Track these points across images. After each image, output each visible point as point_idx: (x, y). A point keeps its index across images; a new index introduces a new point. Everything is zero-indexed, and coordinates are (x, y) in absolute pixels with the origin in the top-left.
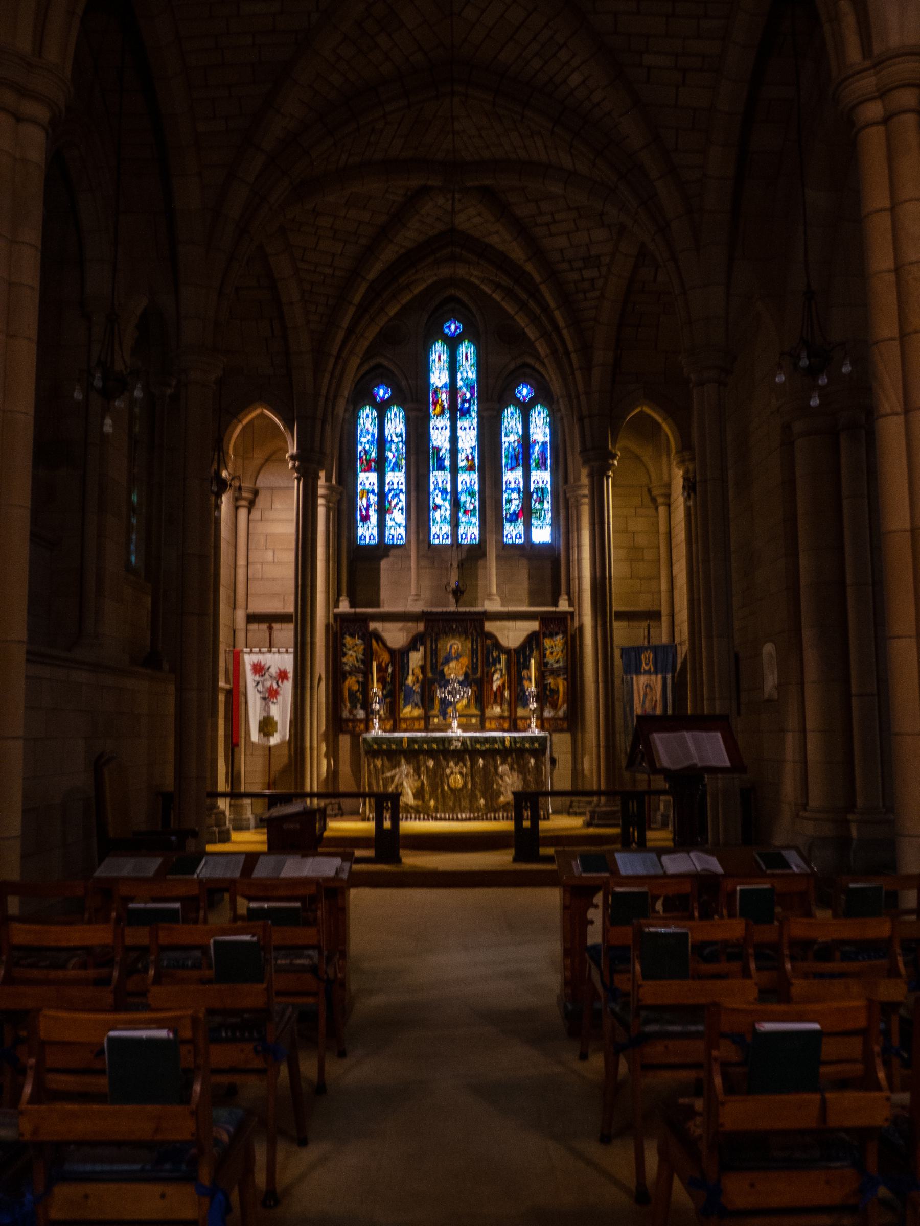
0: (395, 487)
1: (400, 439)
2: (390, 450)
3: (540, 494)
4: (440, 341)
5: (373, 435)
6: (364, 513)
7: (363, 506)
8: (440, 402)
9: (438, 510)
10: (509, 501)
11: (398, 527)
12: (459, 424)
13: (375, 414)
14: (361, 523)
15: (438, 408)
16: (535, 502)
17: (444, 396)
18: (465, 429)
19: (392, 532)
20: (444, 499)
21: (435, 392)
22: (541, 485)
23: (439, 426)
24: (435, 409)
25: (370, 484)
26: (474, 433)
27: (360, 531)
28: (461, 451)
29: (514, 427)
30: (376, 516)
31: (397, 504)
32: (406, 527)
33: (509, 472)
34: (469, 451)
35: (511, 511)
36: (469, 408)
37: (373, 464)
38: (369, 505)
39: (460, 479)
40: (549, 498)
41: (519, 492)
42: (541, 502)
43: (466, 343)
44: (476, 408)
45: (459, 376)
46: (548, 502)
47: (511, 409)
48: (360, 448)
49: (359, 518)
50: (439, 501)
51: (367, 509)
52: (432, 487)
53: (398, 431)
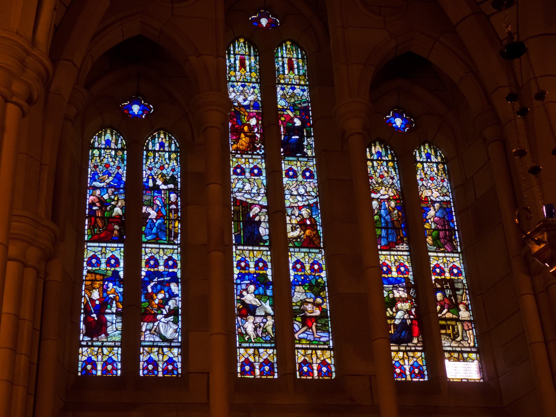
0: (161, 268)
1: (171, 186)
2: (151, 205)
3: (448, 292)
4: (242, 40)
5: (118, 177)
6: (94, 315)
7: (92, 301)
8: (246, 128)
9: (251, 319)
10: (393, 302)
11: (165, 350)
12: (285, 167)
13: (122, 142)
14: (87, 339)
15: (244, 140)
16: (442, 309)
17: (253, 122)
18: (295, 175)
19: (154, 356)
20: (259, 296)
21: (237, 114)
22: (447, 275)
23: (247, 167)
24: (237, 141)
25: (108, 263)
26: (311, 186)
27: (84, 354)
28: (289, 211)
29: (386, 175)
30: (119, 326)
31: (165, 302)
32: (184, 348)
33: (388, 253)
34: (305, 212)
35: (397, 322)
36: (301, 140)
37: (116, 227)
38: (105, 302)
39: (292, 260)
40: (466, 298)
41: (407, 289)
42: (454, 307)
43: (289, 46)
44: (311, 141)
45: (280, 92)
46: (467, 309)
47: (377, 148)
48: (90, 199)
49: (82, 326)
50: (250, 298)
51: (101, 309)
52: (236, 271)
53: (168, 171)
